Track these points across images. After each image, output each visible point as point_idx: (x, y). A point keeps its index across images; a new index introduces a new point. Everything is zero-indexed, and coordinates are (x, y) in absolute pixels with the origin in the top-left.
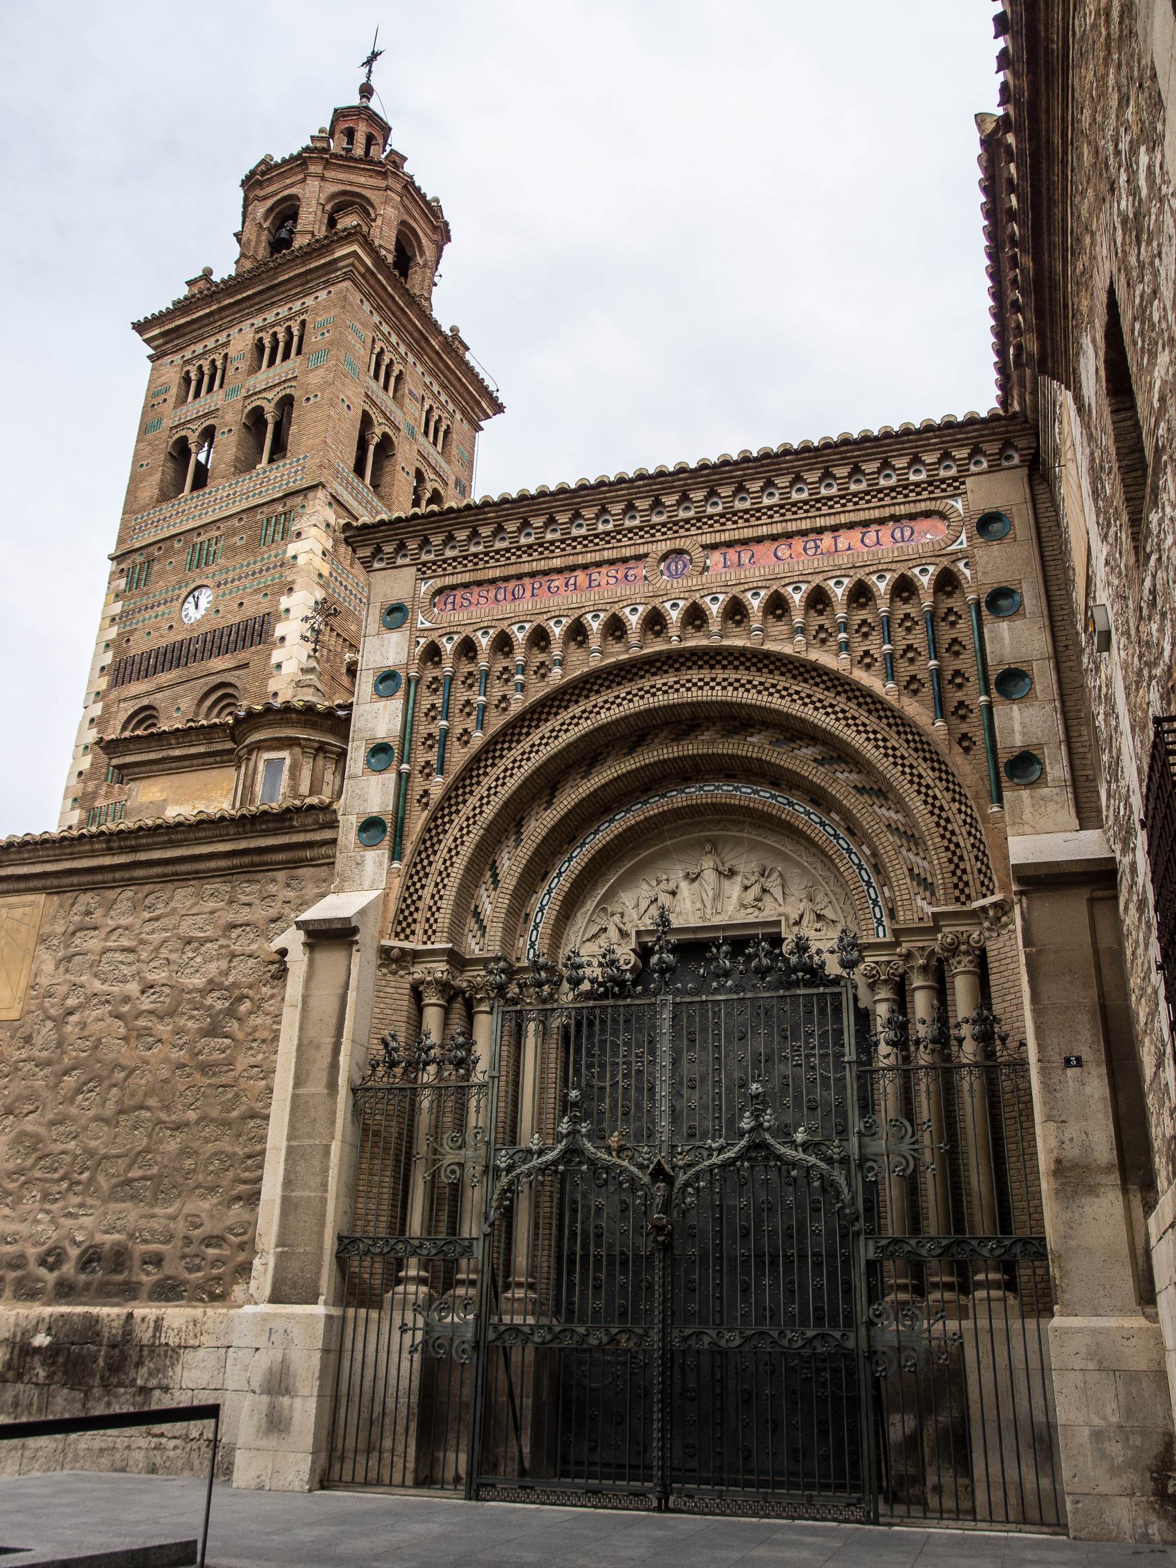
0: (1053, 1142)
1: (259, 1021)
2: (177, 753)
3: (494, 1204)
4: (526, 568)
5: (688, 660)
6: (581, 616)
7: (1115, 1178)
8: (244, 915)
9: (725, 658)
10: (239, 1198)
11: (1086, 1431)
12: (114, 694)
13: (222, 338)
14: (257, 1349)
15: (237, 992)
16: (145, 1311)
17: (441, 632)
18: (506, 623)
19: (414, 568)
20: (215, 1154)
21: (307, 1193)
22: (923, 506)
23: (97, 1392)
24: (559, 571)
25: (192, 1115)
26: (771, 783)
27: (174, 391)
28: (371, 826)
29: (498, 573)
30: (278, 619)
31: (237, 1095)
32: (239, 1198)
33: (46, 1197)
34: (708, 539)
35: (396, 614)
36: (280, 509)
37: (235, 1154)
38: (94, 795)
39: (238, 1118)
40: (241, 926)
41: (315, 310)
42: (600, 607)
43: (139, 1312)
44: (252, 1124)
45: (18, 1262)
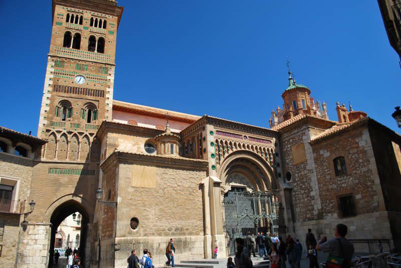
2: (122, 128)
12: (55, 93)
13: (81, 11)
16: (188, 237)
23: (183, 249)
24: (231, 134)
25: (189, 207)
27: (65, 17)
28: (213, 167)
30: (106, 93)
33: (166, 219)
36: (104, 66)
38: (52, 118)
41: (109, 19)
43: (187, 237)
45: (164, 230)
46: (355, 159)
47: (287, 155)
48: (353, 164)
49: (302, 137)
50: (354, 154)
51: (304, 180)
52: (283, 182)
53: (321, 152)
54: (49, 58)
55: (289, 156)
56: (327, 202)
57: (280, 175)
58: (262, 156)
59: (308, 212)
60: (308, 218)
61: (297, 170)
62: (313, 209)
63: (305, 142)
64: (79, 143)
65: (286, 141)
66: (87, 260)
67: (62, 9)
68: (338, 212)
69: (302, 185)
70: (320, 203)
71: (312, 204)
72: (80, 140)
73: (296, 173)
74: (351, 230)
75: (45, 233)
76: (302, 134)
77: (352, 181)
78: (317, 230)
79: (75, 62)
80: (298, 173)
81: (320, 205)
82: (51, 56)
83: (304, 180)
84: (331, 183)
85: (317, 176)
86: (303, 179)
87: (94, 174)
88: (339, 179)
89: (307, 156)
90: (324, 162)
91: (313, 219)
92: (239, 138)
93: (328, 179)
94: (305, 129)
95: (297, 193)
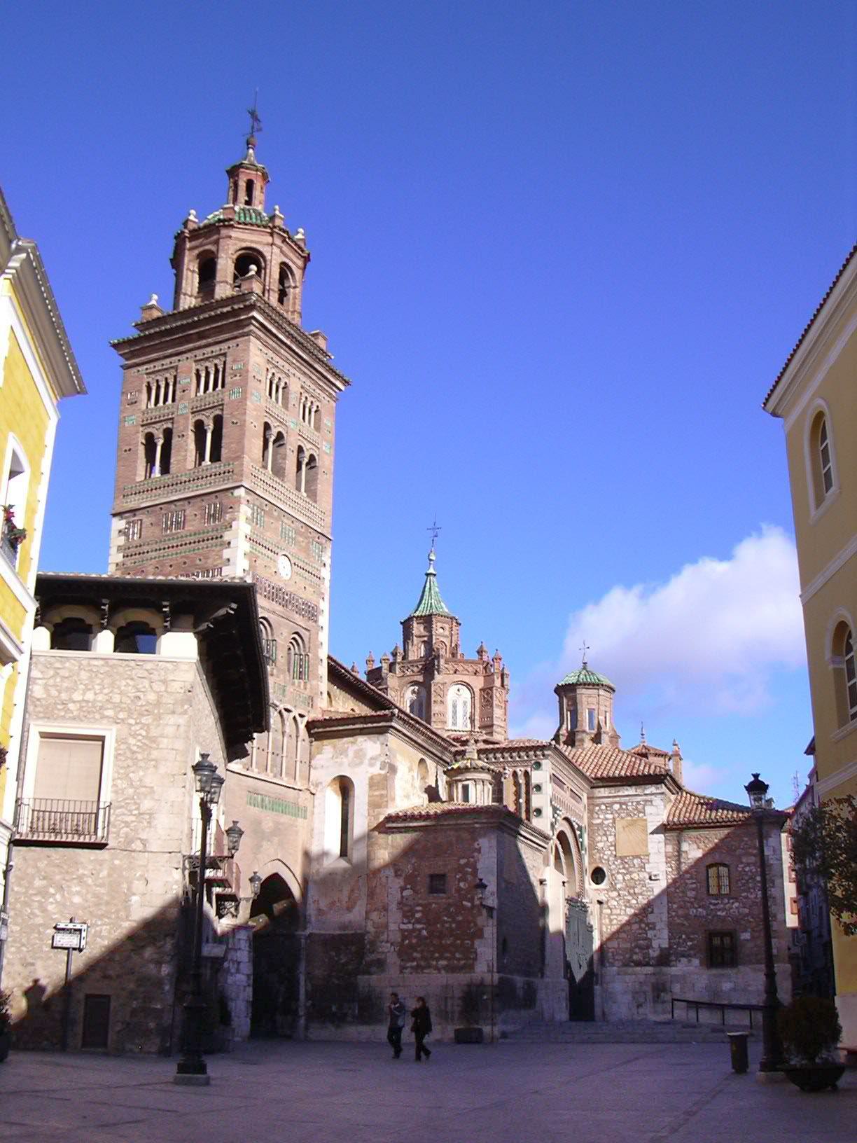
27: (263, 379)
46: (749, 873)
47: (601, 832)
48: (743, 881)
49: (644, 806)
50: (748, 865)
54: (241, 492)
55: (605, 835)
56: (680, 937)
59: (637, 950)
61: (624, 868)
62: (649, 947)
63: (649, 818)
64: (283, 733)
65: (604, 804)
66: (301, 1013)
67: (259, 352)
69: (630, 898)
70: (666, 937)
71: (649, 936)
72: (287, 730)
73: (618, 873)
74: (724, 988)
75: (247, 949)
76: (646, 801)
77: (737, 908)
78: (653, 984)
79: (278, 519)
82: (249, 490)
84: (696, 906)
86: (634, 888)
87: (305, 818)
88: (713, 901)
89: (650, 846)
91: (648, 964)
93: (690, 898)
94: (652, 794)
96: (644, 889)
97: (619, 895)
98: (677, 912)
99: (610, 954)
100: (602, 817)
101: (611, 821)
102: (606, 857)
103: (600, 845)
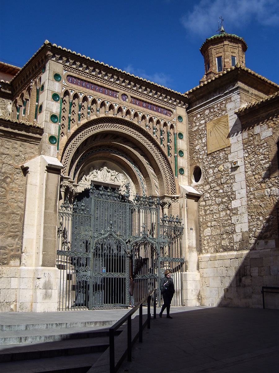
0: (188, 243)
1: (13, 185)
3: (94, 245)
4: (91, 81)
5: (125, 122)
6: (104, 101)
7: (195, 250)
8: (6, 151)
9: (132, 125)
10: (10, 236)
11: (191, 290)
14: (39, 278)
15: (6, 175)
17: (70, 88)
18: (87, 94)
19: (62, 65)
20: (2, 223)
21: (50, 239)
22: (169, 108)
24: (98, 85)
26: (126, 155)
28: (52, 139)
29: (84, 78)
31: (8, 206)
32: (10, 236)
34: (132, 95)
35: (57, 77)
37: (8, 223)
39: (8, 213)
40: (6, 154)
42: (109, 101)
44: (13, 216)
47: (197, 137)
51: (223, 180)
52: (187, 183)
53: (257, 129)
56: (258, 219)
57: (182, 170)
58: (154, 133)
59: (225, 236)
60: (222, 247)
61: (214, 163)
62: (234, 232)
68: (277, 237)
73: (210, 168)
80: (213, 168)
81: (247, 224)
83: (223, 180)
84: (271, 185)
85: (246, 172)
90: (261, 148)
91: (232, 249)
92: (112, 96)
95: (209, 202)
96: (228, 177)
97: (211, 187)
98: (254, 194)
99: (205, 242)
100: (198, 124)
101: (204, 125)
102: (201, 157)
103: (197, 148)
